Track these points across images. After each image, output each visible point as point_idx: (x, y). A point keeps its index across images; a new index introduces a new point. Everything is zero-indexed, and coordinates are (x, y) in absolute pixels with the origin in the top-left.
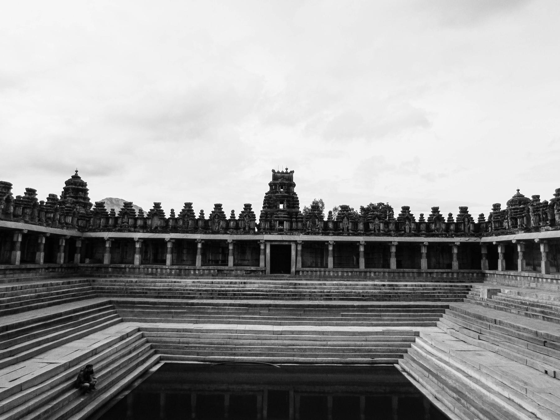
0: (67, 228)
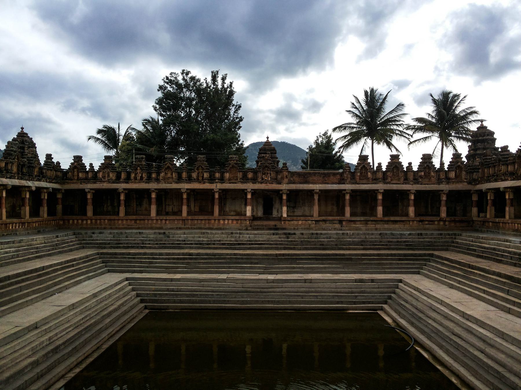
0: (448, 183)
